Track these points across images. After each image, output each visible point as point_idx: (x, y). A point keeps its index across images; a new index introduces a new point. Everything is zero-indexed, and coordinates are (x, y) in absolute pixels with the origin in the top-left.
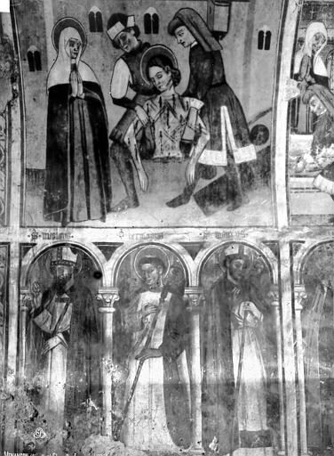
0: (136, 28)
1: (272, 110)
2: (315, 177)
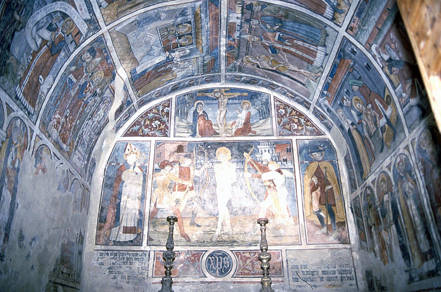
1: (385, 87)
2: (409, 102)
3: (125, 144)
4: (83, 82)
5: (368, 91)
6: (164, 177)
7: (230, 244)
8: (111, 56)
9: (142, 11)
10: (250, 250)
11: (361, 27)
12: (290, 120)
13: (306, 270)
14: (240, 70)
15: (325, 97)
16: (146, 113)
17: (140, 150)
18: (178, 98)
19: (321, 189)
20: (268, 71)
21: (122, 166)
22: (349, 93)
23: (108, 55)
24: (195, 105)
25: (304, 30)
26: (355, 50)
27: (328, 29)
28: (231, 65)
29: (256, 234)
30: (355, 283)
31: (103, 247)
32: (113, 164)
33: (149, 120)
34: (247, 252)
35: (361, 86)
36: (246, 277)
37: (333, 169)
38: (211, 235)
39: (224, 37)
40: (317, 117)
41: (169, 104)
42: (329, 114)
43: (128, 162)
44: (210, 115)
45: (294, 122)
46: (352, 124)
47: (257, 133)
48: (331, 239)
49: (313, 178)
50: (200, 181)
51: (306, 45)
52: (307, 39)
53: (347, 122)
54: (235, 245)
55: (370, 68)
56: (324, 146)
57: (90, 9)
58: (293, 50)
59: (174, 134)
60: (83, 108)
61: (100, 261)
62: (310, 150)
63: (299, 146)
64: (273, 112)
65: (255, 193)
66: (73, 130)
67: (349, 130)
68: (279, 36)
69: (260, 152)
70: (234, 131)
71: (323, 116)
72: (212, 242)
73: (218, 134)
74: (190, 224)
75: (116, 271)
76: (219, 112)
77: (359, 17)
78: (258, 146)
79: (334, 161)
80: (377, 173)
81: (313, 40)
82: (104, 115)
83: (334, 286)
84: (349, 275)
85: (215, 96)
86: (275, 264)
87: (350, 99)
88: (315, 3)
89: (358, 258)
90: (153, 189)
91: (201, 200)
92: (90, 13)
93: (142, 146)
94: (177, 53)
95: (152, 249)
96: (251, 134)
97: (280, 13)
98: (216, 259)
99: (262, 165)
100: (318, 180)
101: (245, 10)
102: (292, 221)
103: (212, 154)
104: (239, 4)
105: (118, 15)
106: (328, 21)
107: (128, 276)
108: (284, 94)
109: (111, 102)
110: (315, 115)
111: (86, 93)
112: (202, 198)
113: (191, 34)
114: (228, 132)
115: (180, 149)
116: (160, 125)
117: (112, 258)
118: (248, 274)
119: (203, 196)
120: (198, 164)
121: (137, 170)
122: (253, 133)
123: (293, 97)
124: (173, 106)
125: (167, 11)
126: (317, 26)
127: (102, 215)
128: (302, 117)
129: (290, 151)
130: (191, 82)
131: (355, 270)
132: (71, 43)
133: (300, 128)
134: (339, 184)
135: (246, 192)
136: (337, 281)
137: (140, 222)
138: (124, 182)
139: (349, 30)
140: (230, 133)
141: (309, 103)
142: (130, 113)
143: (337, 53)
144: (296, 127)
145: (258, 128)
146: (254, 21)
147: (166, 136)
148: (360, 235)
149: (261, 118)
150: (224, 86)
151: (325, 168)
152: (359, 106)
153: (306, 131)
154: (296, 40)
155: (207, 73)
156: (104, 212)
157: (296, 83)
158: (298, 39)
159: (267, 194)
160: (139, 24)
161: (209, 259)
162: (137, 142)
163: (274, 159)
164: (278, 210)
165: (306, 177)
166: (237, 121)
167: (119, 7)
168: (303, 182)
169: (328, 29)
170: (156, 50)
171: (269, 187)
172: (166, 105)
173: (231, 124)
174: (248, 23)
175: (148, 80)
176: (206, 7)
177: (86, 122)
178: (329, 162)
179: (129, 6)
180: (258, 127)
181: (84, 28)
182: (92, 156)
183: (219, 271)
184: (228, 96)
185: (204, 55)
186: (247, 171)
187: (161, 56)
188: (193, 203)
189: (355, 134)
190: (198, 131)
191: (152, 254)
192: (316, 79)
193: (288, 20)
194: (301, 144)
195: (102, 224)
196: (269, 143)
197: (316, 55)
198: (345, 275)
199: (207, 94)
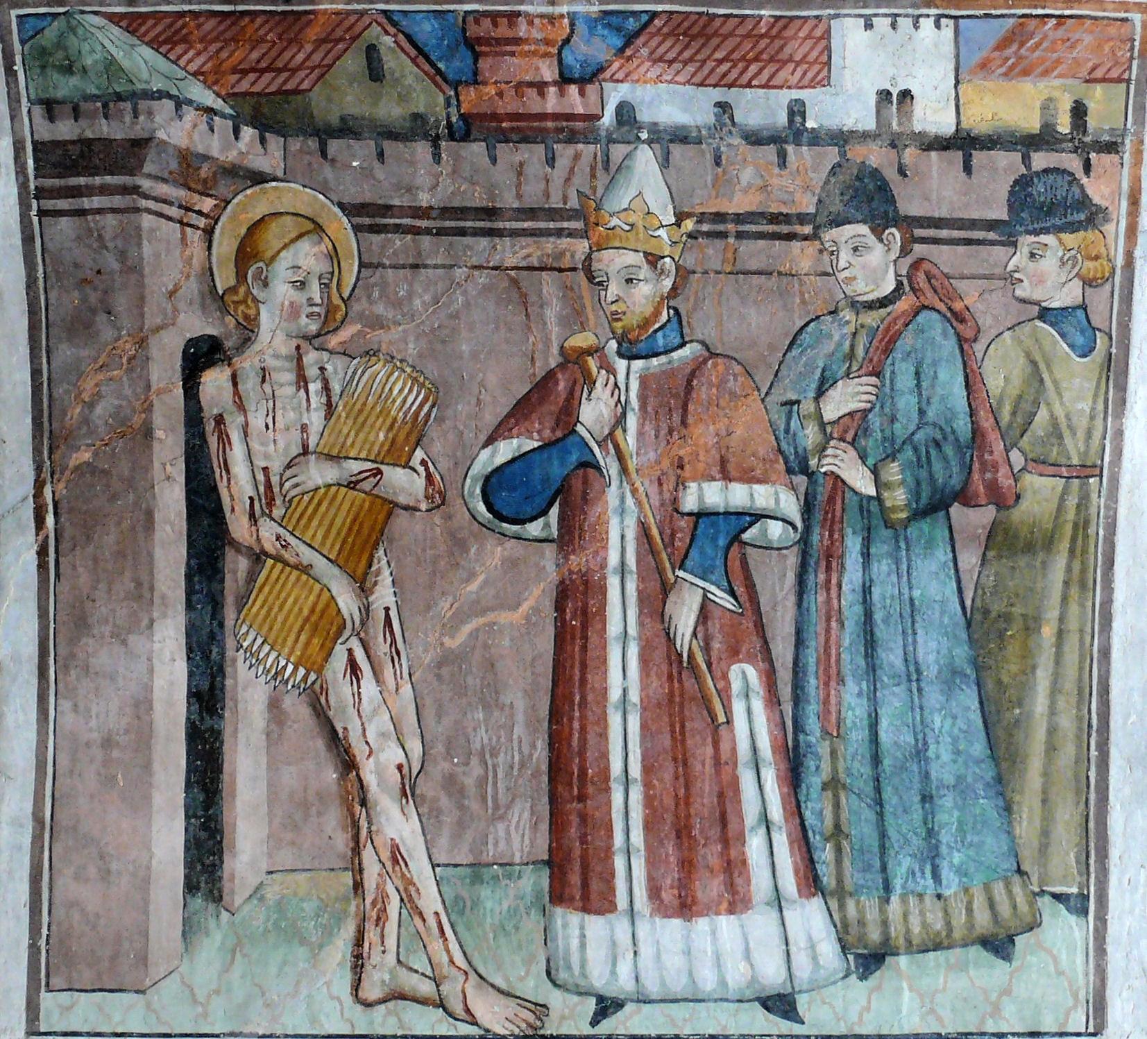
27: (1063, 932)
51: (761, 792)
81: (862, 827)
97: (1032, 481)
126: (1026, 827)
158: (789, 698)
169: (1063, 932)
174: (836, 206)
193: (969, 559)
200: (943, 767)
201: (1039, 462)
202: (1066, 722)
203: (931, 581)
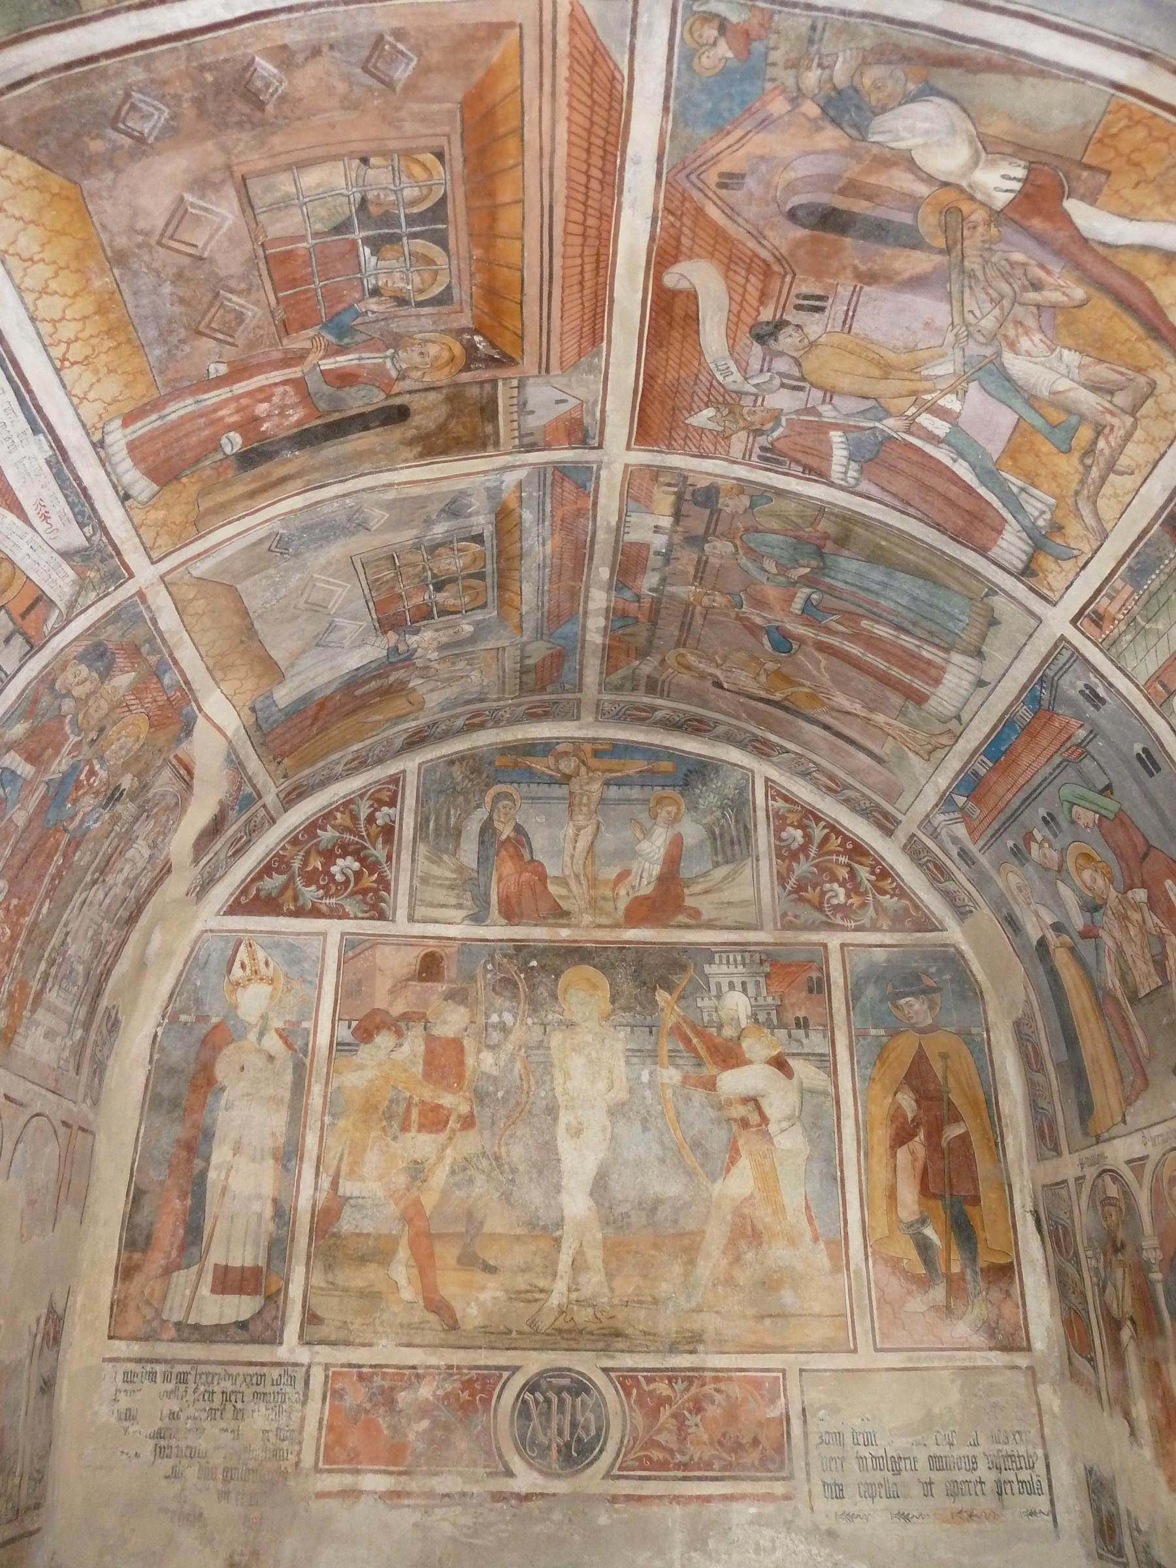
0: (1044, 839)
3: (232, 944)
4: (64, 767)
5: (1139, 841)
6: (369, 1074)
7: (601, 1345)
8: (176, 662)
9: (297, 502)
10: (673, 1370)
11: (1139, 619)
12: (823, 867)
13: (873, 1450)
14: (652, 687)
15: (957, 815)
16: (312, 827)
17: (285, 969)
18: (426, 770)
19: (929, 1136)
20: (753, 703)
21: (216, 1027)
22: (1057, 825)
23: (162, 661)
24: (488, 799)
25: (905, 592)
26: (1101, 691)
28: (621, 673)
29: (693, 1304)
30: (1046, 1508)
31: (136, 1349)
32: (183, 1018)
33: (320, 853)
34: (661, 1378)
35: (1112, 816)
36: (656, 1478)
37: (970, 1060)
38: (534, 1307)
39: (601, 588)
40: (920, 866)
41: (395, 793)
42: (965, 867)
43: (241, 1012)
44: (539, 840)
45: (834, 879)
46: (1058, 928)
47: (705, 917)
48: (962, 1329)
49: (899, 1096)
50: (500, 1094)
51: (907, 641)
52: (914, 624)
53: (1038, 916)
54: (620, 1346)
55: (1158, 769)
56: (940, 972)
57: (82, 513)
58: (855, 650)
59: (412, 908)
60: (65, 856)
61: (124, 1402)
62: (890, 988)
63: (852, 972)
64: (763, 838)
65: (696, 1145)
66: (28, 941)
67: (1042, 942)
68: (808, 598)
69: (714, 992)
70: (622, 905)
71: (940, 868)
72: (537, 1333)
73: (566, 914)
74: (459, 1260)
75: (183, 1444)
76: (571, 832)
77: (1137, 586)
78: (706, 967)
79: (974, 1031)
80: (1153, 1139)
81: (934, 628)
82: (151, 857)
83: (971, 1516)
84: (1024, 1475)
85: (558, 771)
86: (760, 1425)
87: (1058, 847)
88: (959, 507)
89: (1056, 1409)
90: (327, 1119)
91: (500, 1166)
92: (81, 526)
93: (293, 954)
94: (427, 635)
95: (317, 1359)
96: (682, 918)
98: (548, 1401)
99: (718, 1040)
100: (917, 1101)
101: (686, 508)
102: (822, 1259)
103: (543, 992)
104: (669, 485)
105: (199, 524)
106: (1006, 575)
107: (226, 1470)
108: (805, 775)
109: (180, 806)
110: (912, 859)
111: (75, 801)
112: (505, 1159)
113: (481, 576)
114: (601, 909)
115: (430, 967)
116: (358, 875)
117: (169, 1394)
118: (663, 1465)
119: (508, 1151)
120: (494, 1026)
121: (273, 1043)
122: (690, 916)
123: (835, 788)
124: (407, 801)
125: (395, 500)
126: (956, 587)
127: (138, 1219)
128: (863, 860)
129: (819, 987)
130: (476, 720)
131: (1046, 1457)
132: (7, 641)
133: (855, 900)
134: (991, 1117)
135: (662, 1143)
136: (982, 1499)
137: (279, 1248)
138: (223, 1089)
139: (1084, 622)
140: (608, 915)
141: (894, 818)
142: (253, 831)
143: (1025, 687)
144: (842, 898)
145: (710, 897)
146: (718, 544)
147: (382, 916)
148: (1068, 1324)
149: (720, 858)
150: (591, 734)
151: (944, 1056)
152: (1094, 881)
153: (876, 910)
154: (868, 618)
155: (532, 692)
156: (146, 1210)
157: (852, 749)
158: (878, 618)
159: (737, 1151)
160: (281, 546)
161: (524, 1402)
162: (276, 938)
163: (762, 1017)
164: (775, 1212)
165: (877, 1087)
166: (635, 867)
167: (205, 491)
168: (865, 1108)
169: (998, 602)
170: (350, 629)
171: (744, 1123)
172: (385, 796)
173: (614, 876)
175: (319, 723)
176: (542, 486)
177: (78, 899)
178: (958, 1034)
179: (239, 489)
180: (706, 892)
181: (57, 582)
182: (104, 1002)
183: (559, 1451)
184: (604, 771)
185: (525, 639)
186: (666, 1059)
187: (368, 648)
188: (471, 1181)
189: (1061, 959)
190: (494, 899)
191: (317, 1376)
192: (933, 752)
193: (846, 553)
194: (860, 961)
195: (137, 1256)
196: (747, 955)
197: (942, 677)
198: (1010, 1475)
199: (529, 761)
200: (923, 595)
201: (814, 522)
202: (922, 554)
203: (849, 568)
